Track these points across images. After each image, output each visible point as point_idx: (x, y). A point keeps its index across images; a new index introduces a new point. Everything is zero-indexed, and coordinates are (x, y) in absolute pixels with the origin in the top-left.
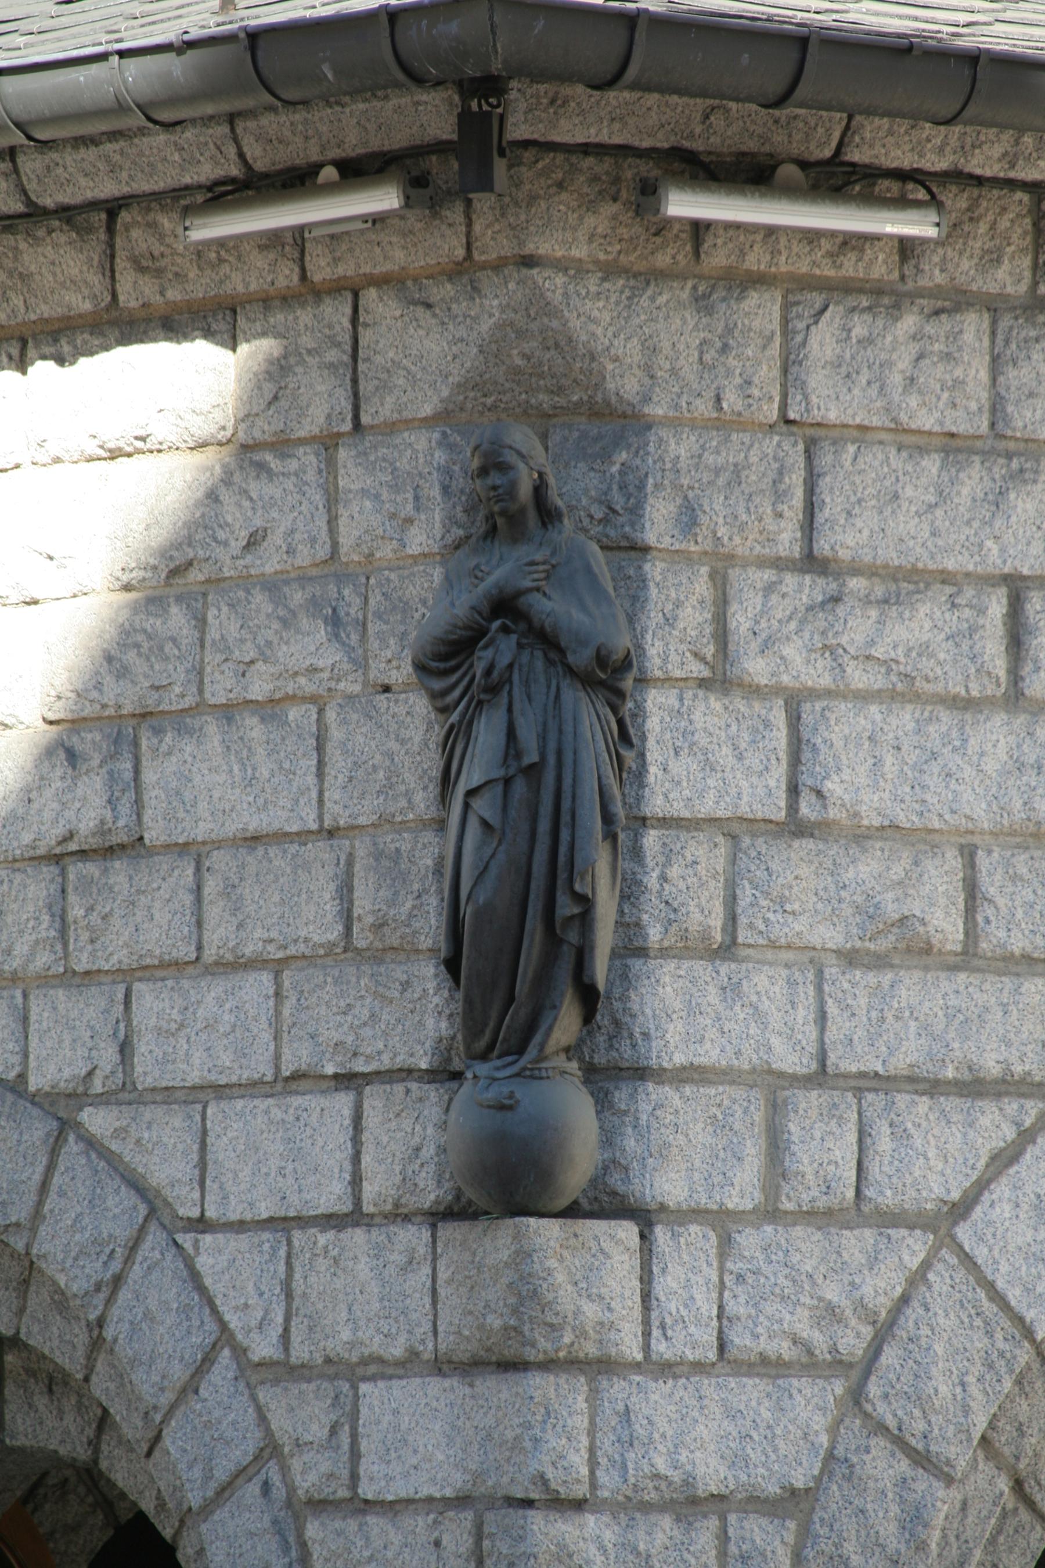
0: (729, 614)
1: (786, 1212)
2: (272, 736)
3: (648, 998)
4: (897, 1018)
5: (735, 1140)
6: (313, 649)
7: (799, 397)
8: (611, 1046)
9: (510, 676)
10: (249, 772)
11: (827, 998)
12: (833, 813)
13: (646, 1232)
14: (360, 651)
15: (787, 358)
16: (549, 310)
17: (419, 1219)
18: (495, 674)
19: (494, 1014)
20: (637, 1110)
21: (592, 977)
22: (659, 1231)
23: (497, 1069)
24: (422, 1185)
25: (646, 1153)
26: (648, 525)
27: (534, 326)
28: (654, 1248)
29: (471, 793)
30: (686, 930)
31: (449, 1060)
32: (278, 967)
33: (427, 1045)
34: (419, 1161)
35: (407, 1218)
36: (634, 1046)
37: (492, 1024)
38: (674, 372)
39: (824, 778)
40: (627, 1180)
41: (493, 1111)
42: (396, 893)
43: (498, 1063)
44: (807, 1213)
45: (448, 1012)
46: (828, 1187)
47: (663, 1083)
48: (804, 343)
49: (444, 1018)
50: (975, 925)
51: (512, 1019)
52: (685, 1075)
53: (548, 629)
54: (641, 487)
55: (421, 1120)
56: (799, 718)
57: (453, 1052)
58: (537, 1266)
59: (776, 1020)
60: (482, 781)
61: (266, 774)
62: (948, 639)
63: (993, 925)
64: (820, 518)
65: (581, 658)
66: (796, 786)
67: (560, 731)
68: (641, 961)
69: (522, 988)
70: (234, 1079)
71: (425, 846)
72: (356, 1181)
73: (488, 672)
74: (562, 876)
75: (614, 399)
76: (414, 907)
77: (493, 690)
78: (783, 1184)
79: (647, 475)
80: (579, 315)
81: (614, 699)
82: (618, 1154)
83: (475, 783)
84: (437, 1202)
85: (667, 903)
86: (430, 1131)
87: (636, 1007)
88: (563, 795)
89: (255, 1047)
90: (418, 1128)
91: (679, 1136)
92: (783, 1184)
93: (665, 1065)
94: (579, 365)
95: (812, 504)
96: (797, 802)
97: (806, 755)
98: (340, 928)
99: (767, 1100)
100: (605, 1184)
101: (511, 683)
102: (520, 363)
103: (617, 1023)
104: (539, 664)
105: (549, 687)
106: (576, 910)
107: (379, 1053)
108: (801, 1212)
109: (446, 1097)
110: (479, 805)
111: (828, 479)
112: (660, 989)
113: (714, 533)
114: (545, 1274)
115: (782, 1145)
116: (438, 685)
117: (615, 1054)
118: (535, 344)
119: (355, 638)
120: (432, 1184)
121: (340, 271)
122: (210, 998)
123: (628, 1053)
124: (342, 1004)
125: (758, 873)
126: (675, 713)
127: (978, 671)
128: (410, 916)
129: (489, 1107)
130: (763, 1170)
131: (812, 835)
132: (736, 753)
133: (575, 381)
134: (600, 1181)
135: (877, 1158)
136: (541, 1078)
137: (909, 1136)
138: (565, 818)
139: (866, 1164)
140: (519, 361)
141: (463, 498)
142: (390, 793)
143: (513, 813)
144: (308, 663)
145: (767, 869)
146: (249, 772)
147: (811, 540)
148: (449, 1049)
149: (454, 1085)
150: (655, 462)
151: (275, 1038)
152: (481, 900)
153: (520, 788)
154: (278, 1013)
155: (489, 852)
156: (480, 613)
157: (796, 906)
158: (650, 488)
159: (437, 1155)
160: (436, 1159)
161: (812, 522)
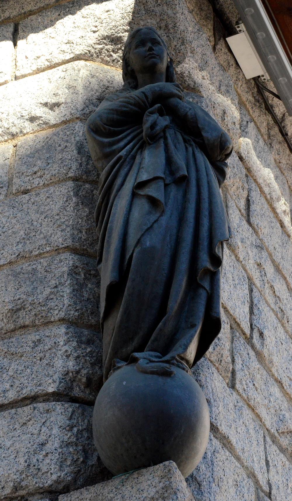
12: (265, 352)
23: (152, 356)
24: (44, 469)
25: (211, 480)
27: (157, 9)
31: (71, 388)
33: (56, 377)
34: (44, 453)
42: (35, 288)
45: (76, 355)
51: (165, 324)
55: (48, 424)
57: (75, 384)
64: (253, 207)
69: (173, 305)
74: (204, 243)
76: (51, 293)
83: (144, 177)
84: (57, 482)
90: (44, 429)
94: (175, 43)
97: (255, 311)
109: (70, 410)
121: (7, 14)
142: (28, 242)
148: (73, 381)
155: (153, 218)
159: (61, 447)
160: (60, 450)
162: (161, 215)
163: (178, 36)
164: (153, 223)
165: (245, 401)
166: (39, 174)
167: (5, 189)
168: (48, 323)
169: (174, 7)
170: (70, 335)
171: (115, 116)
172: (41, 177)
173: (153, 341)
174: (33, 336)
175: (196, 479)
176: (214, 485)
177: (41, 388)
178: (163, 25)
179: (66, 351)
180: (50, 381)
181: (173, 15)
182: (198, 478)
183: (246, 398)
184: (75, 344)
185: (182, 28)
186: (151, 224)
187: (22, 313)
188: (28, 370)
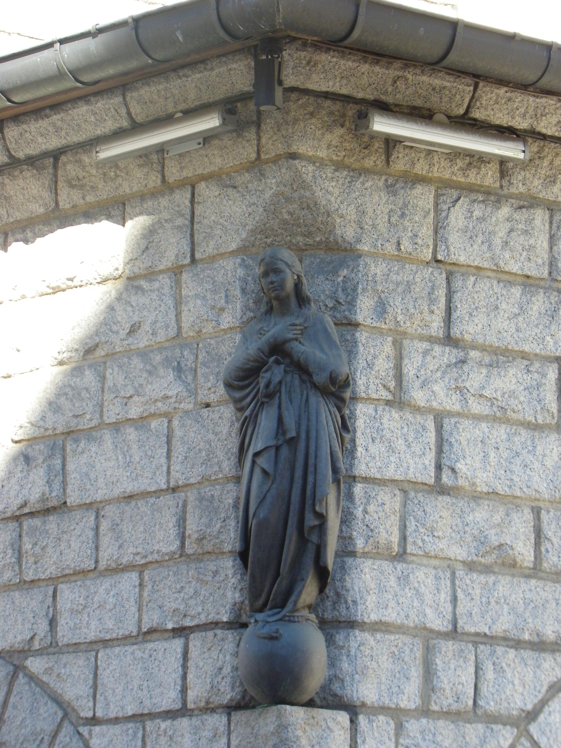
0: (403, 365)
1: (434, 712)
2: (141, 438)
3: (356, 581)
4: (497, 603)
5: (405, 667)
6: (166, 385)
7: (444, 247)
8: (334, 608)
9: (280, 388)
10: (128, 458)
11: (457, 588)
12: (461, 482)
13: (354, 718)
14: (193, 385)
15: (437, 225)
16: (304, 185)
17: (220, 710)
18: (272, 387)
19: (267, 584)
20: (349, 646)
21: (325, 562)
22: (361, 718)
23: (269, 616)
24: (222, 690)
25: (354, 672)
26: (358, 311)
27: (296, 195)
28: (358, 728)
29: (257, 455)
30: (378, 542)
31: (240, 616)
32: (141, 569)
33: (227, 607)
34: (221, 676)
35: (213, 710)
36: (348, 608)
37: (266, 590)
38: (374, 226)
39: (456, 461)
40: (343, 687)
41: (266, 640)
42: (211, 520)
43: (270, 613)
44: (446, 713)
45: (240, 587)
46: (458, 698)
47: (364, 631)
48: (447, 217)
49: (237, 590)
50: (540, 553)
51: (278, 585)
52: (377, 627)
53: (302, 362)
54: (355, 289)
55: (223, 651)
56: (442, 427)
57: (242, 612)
58: (290, 734)
59: (428, 598)
60: (263, 448)
61: (138, 459)
62: (525, 389)
63: (550, 553)
64: (454, 316)
65: (320, 378)
66: (440, 465)
67: (309, 420)
68: (352, 559)
69: (284, 568)
70: (114, 636)
71: (228, 492)
72: (184, 690)
73: (267, 386)
74: (309, 502)
75: (340, 240)
76: (221, 527)
77: (270, 396)
78: (432, 694)
79: (358, 283)
80: (321, 189)
81: (339, 403)
82: (338, 672)
83: (259, 447)
84: (231, 700)
85: (367, 526)
86: (228, 658)
87: (349, 585)
88: (310, 456)
89: (127, 616)
90: (221, 656)
91: (373, 663)
92: (432, 694)
93: (366, 620)
94: (320, 219)
95: (450, 308)
96: (440, 474)
97: (446, 448)
98: (178, 543)
99: (424, 645)
100: (330, 689)
101: (280, 392)
102: (287, 217)
103: (338, 594)
104: (297, 382)
105: (302, 395)
106: (317, 523)
107: (199, 614)
108: (443, 712)
109: (238, 638)
110: (262, 461)
111: (459, 294)
112: (363, 575)
113: (396, 318)
114: (295, 739)
115: (432, 672)
116: (238, 395)
117: (337, 613)
118: (296, 206)
119: (190, 378)
120: (228, 689)
121: (185, 174)
122: (101, 590)
123: (344, 612)
124: (178, 587)
125: (419, 513)
126: (372, 418)
127: (542, 408)
128: (220, 532)
129: (264, 638)
130: (421, 686)
131: (449, 494)
132: (407, 443)
133: (318, 229)
134: (327, 688)
135: (486, 683)
136: (295, 622)
137: (504, 671)
138: (311, 469)
139: (479, 685)
140: (286, 216)
141: (253, 295)
142: (209, 463)
143: (280, 466)
144: (163, 393)
145: (424, 511)
146: (128, 458)
147: (449, 328)
148: (240, 610)
149: (242, 630)
150: (363, 276)
151: (139, 610)
152: (261, 516)
153: (285, 452)
154: (141, 596)
155: (266, 488)
156: (263, 353)
157: (440, 534)
158: (360, 290)
159: (232, 672)
160: (231, 674)
161: (450, 318)
162: (273, 483)
166: (212, 390)
167: (193, 397)
168: (223, 553)
169: (310, 188)
170: (236, 567)
172: (215, 392)
173: (272, 600)
174: (212, 567)
175: (339, 677)
176: (357, 676)
178: (305, 205)
179: (234, 584)
180: (224, 611)
181: (311, 196)
183: (422, 553)
184: (239, 577)
185: (324, 203)
187: (205, 542)
188: (212, 598)
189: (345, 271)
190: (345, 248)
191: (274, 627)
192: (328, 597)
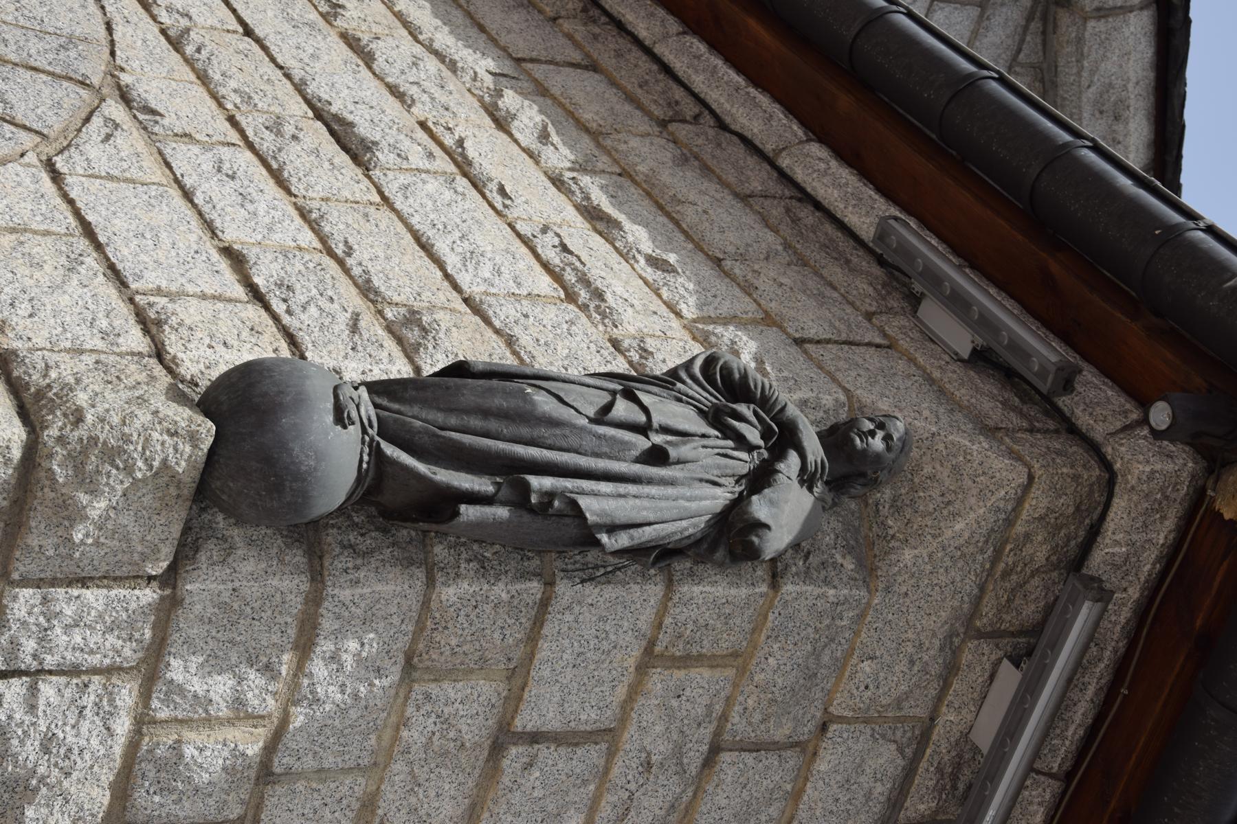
60: (645, 404)
75: (893, 557)
79: (835, 587)
118: (947, 484)
134: (210, 533)
152: (536, 398)
163: (942, 524)
164: (572, 407)
165: (402, 716)
171: (737, 376)
175: (229, 555)
177: (310, 345)
182: (232, 557)
186: (572, 403)
189: (852, 566)
190: (878, 568)
191: (356, 419)
192: (362, 535)
